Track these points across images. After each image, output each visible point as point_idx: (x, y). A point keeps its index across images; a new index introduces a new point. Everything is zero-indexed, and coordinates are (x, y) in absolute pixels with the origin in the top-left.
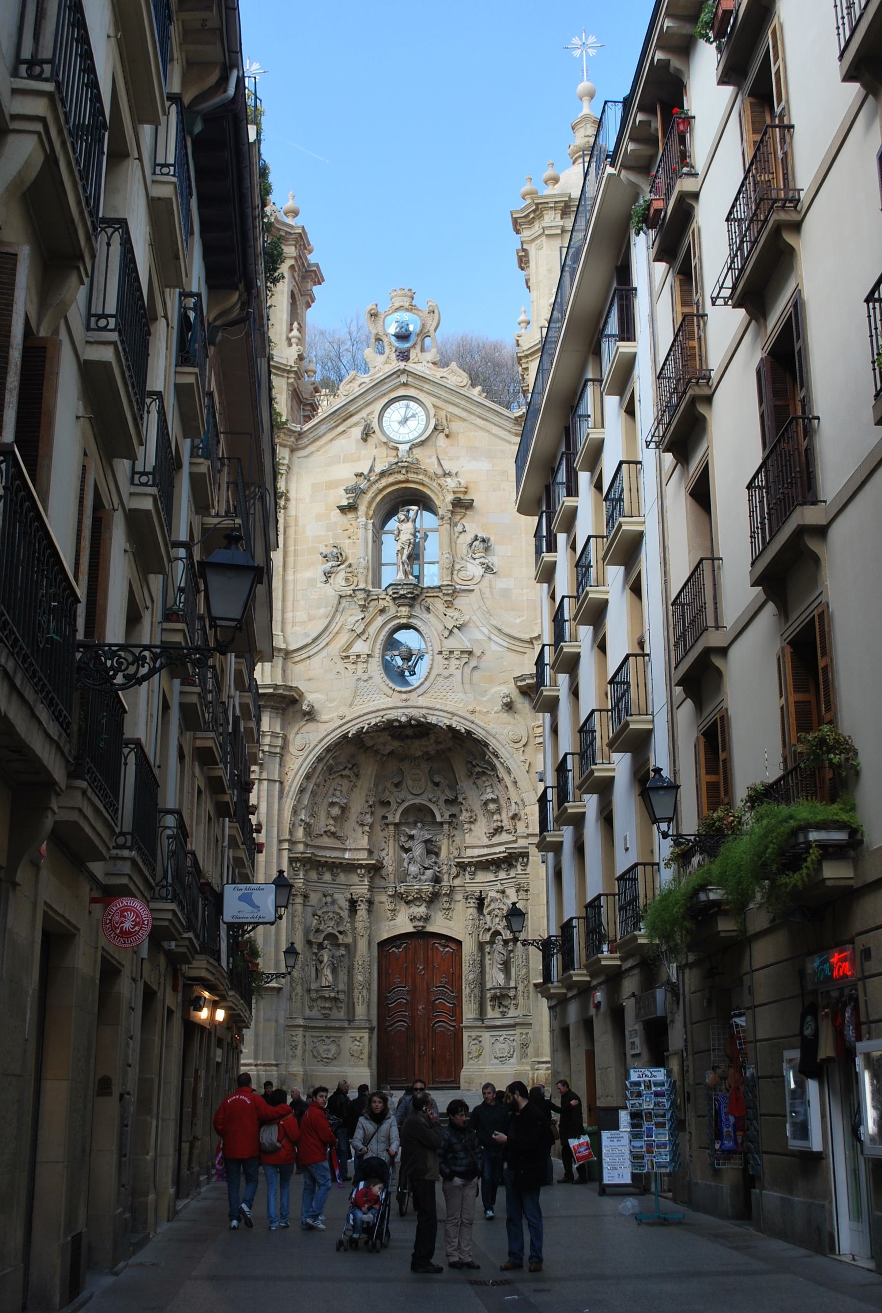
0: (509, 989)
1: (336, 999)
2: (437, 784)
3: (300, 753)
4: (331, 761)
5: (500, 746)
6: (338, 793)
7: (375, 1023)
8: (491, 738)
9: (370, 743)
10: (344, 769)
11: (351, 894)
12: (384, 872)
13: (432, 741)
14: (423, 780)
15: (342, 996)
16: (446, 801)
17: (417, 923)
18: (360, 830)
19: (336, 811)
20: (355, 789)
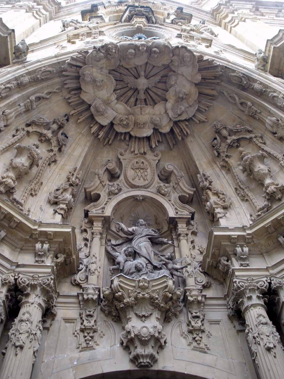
4: (33, 98)
10: (47, 126)
12: (79, 277)
13: (169, 105)
14: (149, 170)
18: (51, 210)
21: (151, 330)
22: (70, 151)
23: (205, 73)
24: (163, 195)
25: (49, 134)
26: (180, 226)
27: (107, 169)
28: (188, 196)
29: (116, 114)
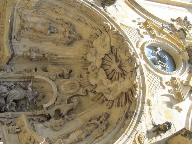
2: (69, 101)
5: (133, 126)
8: (137, 118)
9: (97, 43)
10: (70, 33)
22: (67, 49)
23: (130, 92)
24: (56, 100)
26: (40, 111)
28: (61, 113)
29: (95, 62)
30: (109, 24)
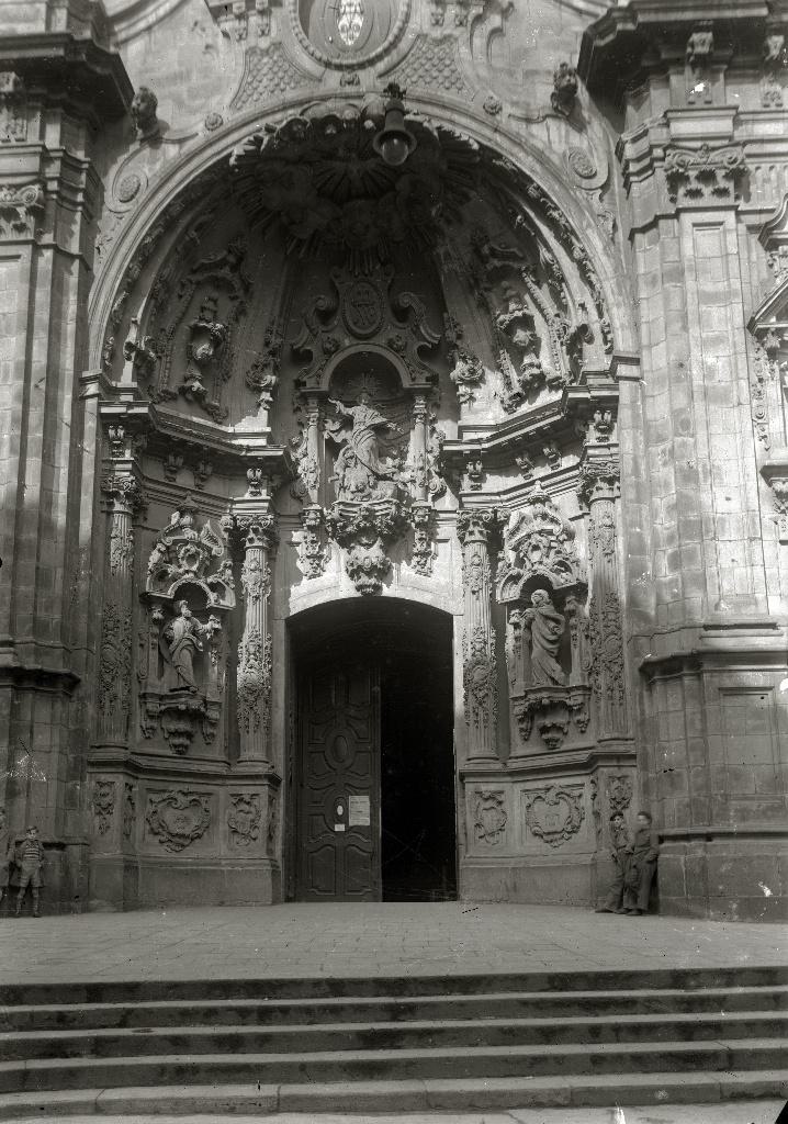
0: (568, 691)
1: (196, 717)
2: (402, 314)
3: (124, 207)
4: (193, 234)
6: (208, 315)
7: (281, 771)
11: (234, 519)
15: (213, 714)
16: (422, 351)
17: (364, 580)
19: (203, 349)
20: (242, 318)
21: (374, 560)
25: (225, 272)
27: (316, 309)
30: (237, 150)
